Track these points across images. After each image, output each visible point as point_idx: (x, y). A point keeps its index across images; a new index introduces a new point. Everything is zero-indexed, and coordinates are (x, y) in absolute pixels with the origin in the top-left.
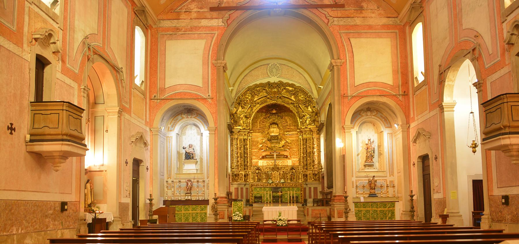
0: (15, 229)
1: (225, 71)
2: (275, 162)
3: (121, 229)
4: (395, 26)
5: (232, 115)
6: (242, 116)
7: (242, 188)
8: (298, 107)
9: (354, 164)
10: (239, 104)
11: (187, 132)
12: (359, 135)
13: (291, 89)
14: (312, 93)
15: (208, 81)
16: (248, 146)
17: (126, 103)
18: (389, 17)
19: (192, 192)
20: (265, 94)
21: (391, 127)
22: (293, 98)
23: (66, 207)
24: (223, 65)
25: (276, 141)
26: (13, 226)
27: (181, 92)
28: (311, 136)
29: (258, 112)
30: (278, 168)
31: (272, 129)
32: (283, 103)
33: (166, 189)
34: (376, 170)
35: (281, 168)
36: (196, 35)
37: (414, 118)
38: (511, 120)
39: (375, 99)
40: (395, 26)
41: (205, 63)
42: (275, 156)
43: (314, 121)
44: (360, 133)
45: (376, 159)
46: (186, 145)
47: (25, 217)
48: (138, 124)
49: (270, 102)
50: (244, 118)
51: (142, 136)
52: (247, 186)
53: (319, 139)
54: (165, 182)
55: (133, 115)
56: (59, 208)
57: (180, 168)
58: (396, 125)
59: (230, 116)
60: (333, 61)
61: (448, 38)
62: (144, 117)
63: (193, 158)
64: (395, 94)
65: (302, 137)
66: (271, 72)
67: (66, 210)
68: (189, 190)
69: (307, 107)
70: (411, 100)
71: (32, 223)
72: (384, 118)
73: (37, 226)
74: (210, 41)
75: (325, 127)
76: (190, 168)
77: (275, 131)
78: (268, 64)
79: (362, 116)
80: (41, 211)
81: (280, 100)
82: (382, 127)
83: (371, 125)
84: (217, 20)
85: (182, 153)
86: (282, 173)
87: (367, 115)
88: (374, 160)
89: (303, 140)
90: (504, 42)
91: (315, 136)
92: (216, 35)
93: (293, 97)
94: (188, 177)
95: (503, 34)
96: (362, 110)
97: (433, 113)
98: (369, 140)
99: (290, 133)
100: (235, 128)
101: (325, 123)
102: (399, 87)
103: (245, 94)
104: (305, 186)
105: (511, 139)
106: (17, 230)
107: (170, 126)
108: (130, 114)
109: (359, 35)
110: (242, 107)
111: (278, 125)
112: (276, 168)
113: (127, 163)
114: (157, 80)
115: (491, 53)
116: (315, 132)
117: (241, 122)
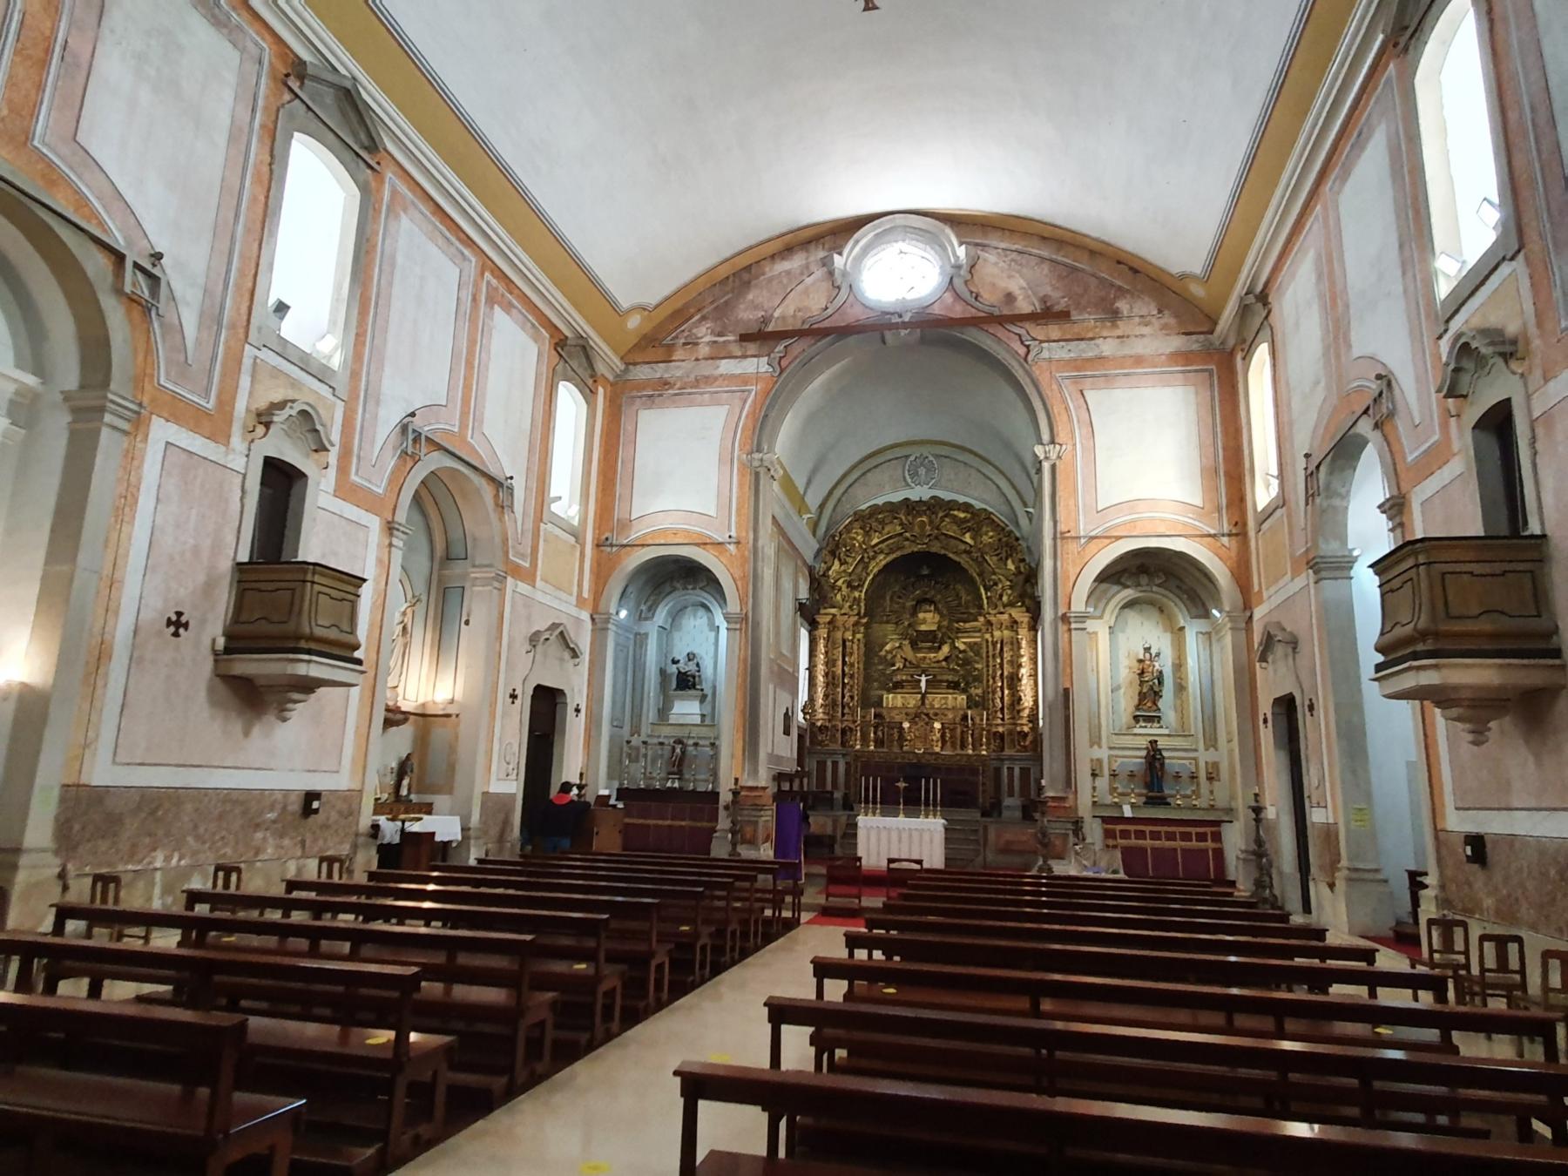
3: (292, 885)
6: (839, 583)
7: (835, 764)
8: (980, 562)
9: (1103, 711)
10: (833, 554)
11: (684, 622)
12: (1121, 637)
13: (962, 515)
17: (523, 556)
19: (685, 771)
21: (1206, 615)
22: (968, 538)
23: (315, 805)
26: (154, 850)
27: (666, 529)
31: (921, 615)
34: (1166, 732)
37: (1260, 591)
40: (1208, 353)
41: (726, 459)
42: (923, 684)
44: (1123, 631)
45: (1167, 702)
46: (681, 657)
47: (196, 827)
49: (910, 548)
55: (539, 583)
56: (295, 806)
57: (663, 712)
58: (1215, 612)
61: (1323, 384)
62: (575, 589)
66: (914, 474)
67: (316, 811)
68: (678, 764)
71: (214, 843)
72: (1185, 592)
73: (228, 851)
74: (737, 410)
76: (687, 709)
80: (244, 813)
82: (1180, 617)
83: (1156, 614)
86: (937, 725)
87: (1139, 585)
88: (1160, 704)
91: (1023, 634)
94: (678, 733)
96: (1125, 570)
97: (1300, 582)
98: (1147, 650)
103: (848, 529)
105: (1445, 672)
106: (168, 859)
107: (644, 608)
108: (532, 582)
109: (1108, 381)
113: (514, 696)
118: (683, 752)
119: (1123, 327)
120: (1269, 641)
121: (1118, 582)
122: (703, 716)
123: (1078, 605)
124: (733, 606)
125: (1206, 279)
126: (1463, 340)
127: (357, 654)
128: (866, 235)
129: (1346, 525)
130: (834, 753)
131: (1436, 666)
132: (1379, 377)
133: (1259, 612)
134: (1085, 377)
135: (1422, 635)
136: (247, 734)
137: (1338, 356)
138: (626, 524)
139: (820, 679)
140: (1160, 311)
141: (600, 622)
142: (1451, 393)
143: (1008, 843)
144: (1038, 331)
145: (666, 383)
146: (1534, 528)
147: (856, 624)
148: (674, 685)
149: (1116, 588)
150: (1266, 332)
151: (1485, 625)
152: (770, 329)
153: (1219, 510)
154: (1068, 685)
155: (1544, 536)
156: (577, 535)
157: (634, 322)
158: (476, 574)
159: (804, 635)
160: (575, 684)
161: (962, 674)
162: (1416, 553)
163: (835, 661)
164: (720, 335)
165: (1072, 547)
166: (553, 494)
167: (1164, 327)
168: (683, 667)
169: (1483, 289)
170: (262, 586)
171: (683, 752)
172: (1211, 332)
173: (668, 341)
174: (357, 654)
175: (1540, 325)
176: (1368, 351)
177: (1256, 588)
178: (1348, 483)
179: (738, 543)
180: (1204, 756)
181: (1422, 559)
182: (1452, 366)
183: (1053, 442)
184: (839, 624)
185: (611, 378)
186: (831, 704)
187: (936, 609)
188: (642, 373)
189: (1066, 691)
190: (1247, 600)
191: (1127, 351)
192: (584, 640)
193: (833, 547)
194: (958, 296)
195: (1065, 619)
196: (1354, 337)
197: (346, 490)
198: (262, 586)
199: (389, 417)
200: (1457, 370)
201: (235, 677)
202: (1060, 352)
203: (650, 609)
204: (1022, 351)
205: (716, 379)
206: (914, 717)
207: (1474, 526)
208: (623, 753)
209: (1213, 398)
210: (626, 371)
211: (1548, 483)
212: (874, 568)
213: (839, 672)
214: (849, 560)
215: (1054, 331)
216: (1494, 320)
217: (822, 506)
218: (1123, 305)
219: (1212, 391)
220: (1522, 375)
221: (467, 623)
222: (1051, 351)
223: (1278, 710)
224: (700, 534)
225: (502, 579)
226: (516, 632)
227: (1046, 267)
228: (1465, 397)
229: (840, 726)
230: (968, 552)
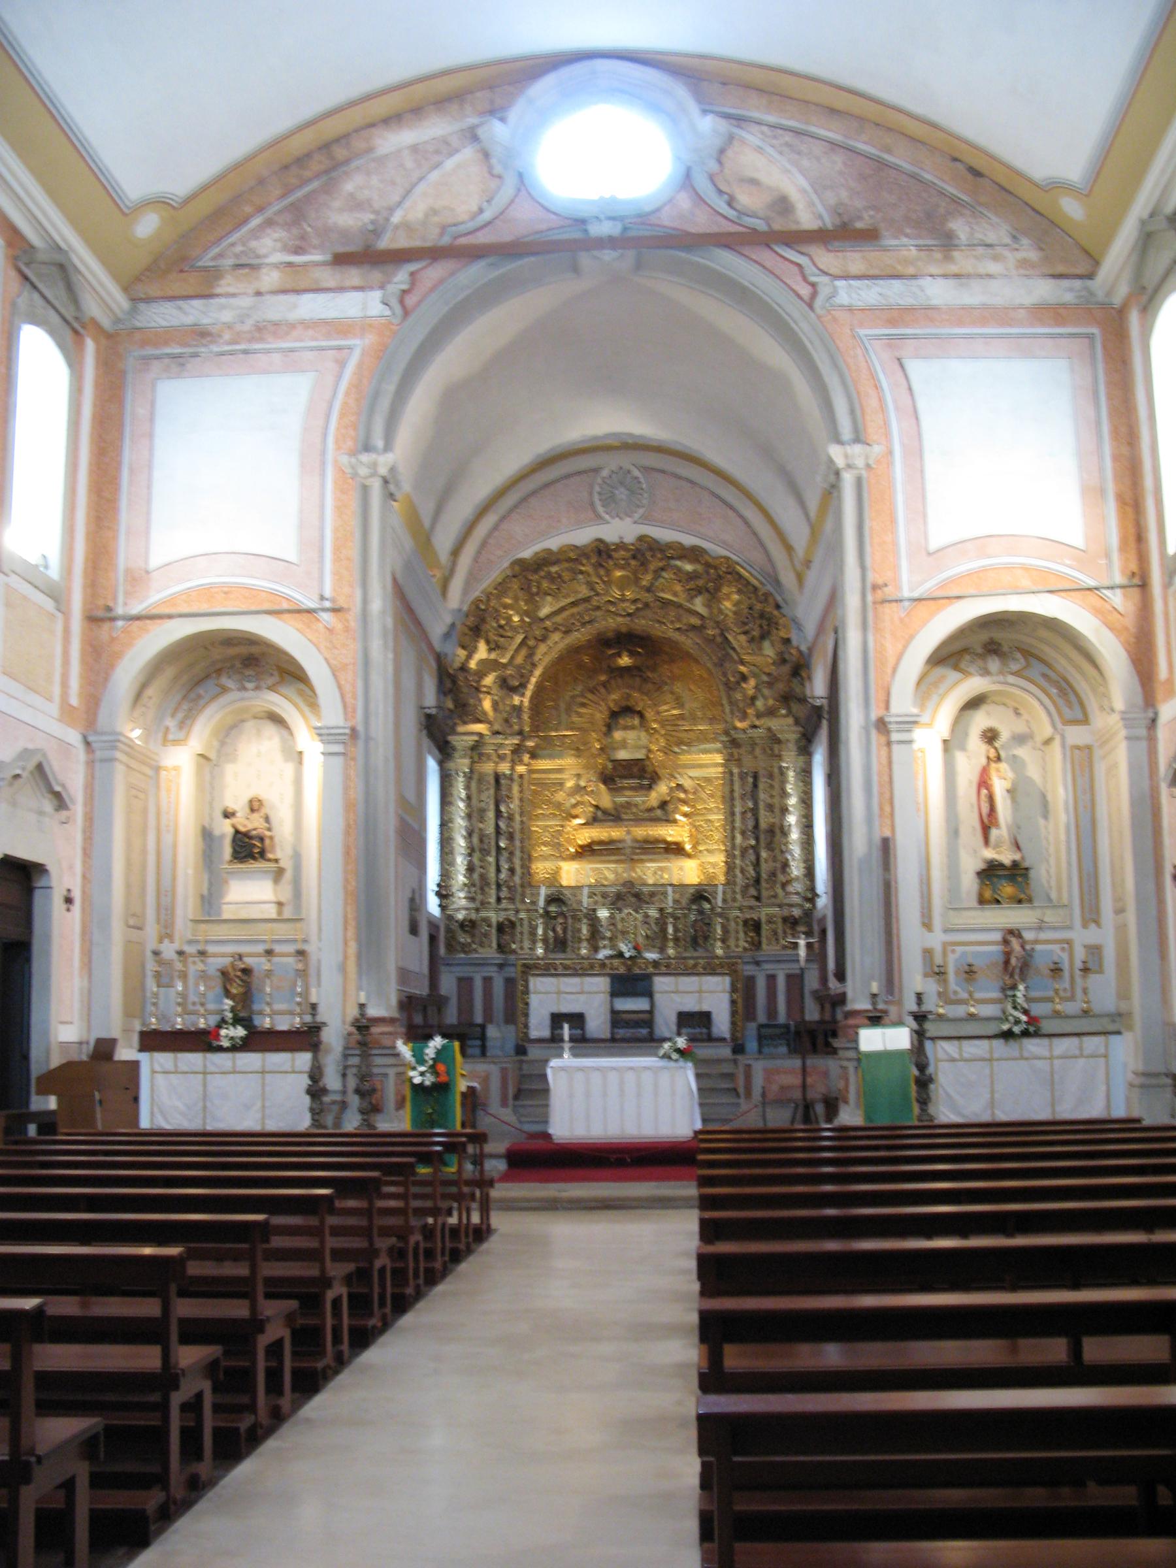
6: (489, 680)
7: (487, 981)
13: (689, 567)
14: (777, 582)
15: (322, 537)
16: (514, 805)
20: (584, 592)
22: (699, 605)
30: (637, 896)
31: (618, 735)
33: (151, 985)
35: (652, 894)
43: (787, 699)
48: (26, 715)
51: (40, 767)
52: (510, 972)
53: (806, 775)
54: (149, 954)
57: (210, 900)
59: (441, 682)
62: (57, 690)
63: (263, 854)
64: (1092, 583)
76: (250, 893)
78: (596, 470)
85: (222, 836)
86: (653, 913)
89: (743, 776)
96: (965, 650)
102: (1108, 556)
104: (749, 970)
107: (171, 723)
110: (488, 642)
112: (630, 896)
116: (792, 746)
121: (956, 667)
122: (280, 904)
123: (902, 703)
124: (332, 714)
125: (1084, 194)
128: (543, 88)
130: (483, 963)
134: (903, 337)
138: (138, 579)
139: (460, 842)
140: (1014, 238)
141: (99, 745)
143: (783, 1088)
144: (826, 258)
147: (517, 750)
148: (227, 851)
149: (954, 675)
152: (384, 243)
154: (887, 833)
156: (57, 594)
157: (147, 226)
159: (432, 765)
163: (482, 811)
164: (298, 250)
165: (890, 613)
167: (1024, 263)
172: (1090, 276)
173: (206, 261)
180: (1082, 937)
183: (858, 439)
184: (489, 750)
185: (106, 323)
186: (478, 884)
192: (72, 777)
194: (699, 199)
195: (882, 725)
202: (869, 294)
204: (805, 291)
205: (292, 326)
210: (134, 311)
212: (546, 654)
213: (490, 830)
215: (855, 259)
217: (456, 552)
218: (960, 227)
222: (852, 290)
224: (272, 594)
227: (839, 159)
229: (494, 917)
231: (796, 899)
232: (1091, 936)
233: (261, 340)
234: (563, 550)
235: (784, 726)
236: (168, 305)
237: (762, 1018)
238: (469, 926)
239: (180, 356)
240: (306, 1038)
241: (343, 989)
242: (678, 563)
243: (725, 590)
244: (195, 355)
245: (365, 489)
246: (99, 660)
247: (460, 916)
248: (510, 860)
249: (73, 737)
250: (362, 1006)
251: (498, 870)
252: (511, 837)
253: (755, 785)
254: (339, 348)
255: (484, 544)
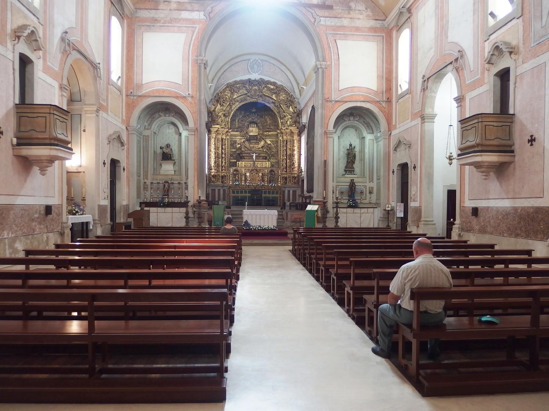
0: (5, 233)
1: (205, 68)
2: (254, 164)
4: (381, 29)
5: (210, 113)
6: (220, 114)
7: (219, 190)
8: (279, 107)
10: (218, 101)
12: (341, 140)
13: (272, 87)
17: (104, 100)
18: (377, 20)
20: (245, 92)
22: (274, 97)
24: (204, 62)
25: (254, 141)
26: (4, 230)
28: (291, 138)
29: (237, 110)
31: (251, 129)
32: (263, 102)
36: (176, 28)
37: (395, 125)
38: (484, 138)
39: (359, 104)
40: (381, 29)
42: (254, 157)
43: (295, 122)
47: (15, 221)
48: (115, 122)
49: (249, 100)
50: (222, 116)
51: (119, 136)
53: (300, 141)
55: (110, 113)
56: (43, 212)
59: (208, 114)
60: (318, 63)
61: (433, 50)
65: (283, 138)
69: (288, 107)
70: (394, 106)
71: (21, 227)
72: (366, 124)
73: (25, 230)
75: (306, 130)
76: (168, 168)
77: (253, 131)
78: (249, 60)
79: (345, 121)
80: (28, 215)
81: (260, 98)
84: (198, 13)
86: (260, 174)
87: (350, 120)
89: (283, 141)
90: (485, 61)
91: (296, 137)
92: (197, 28)
93: (274, 96)
94: (166, 178)
95: (484, 53)
96: (345, 115)
99: (270, 133)
100: (213, 126)
101: (307, 125)
102: (383, 93)
103: (224, 91)
105: (483, 157)
106: (8, 234)
110: (220, 104)
111: (257, 124)
113: (104, 164)
114: (133, 75)
115: (472, 69)
117: (220, 120)
118: (169, 187)
119: (353, 14)
120: (399, 143)
126: (496, 45)
127: (69, 146)
129: (434, 103)
131: (481, 155)
132: (459, 51)
133: (394, 133)
135: (478, 145)
136: (25, 181)
137: (442, 40)
140: (366, 9)
142: (489, 63)
143: (295, 218)
145: (156, 20)
146: (511, 111)
147: (227, 132)
150: (408, 24)
151: (495, 142)
153: (383, 93)
155: (514, 115)
158: (86, 108)
160: (121, 156)
161: (268, 154)
162: (478, 118)
166: (112, 70)
168: (165, 150)
169: (505, 27)
170: (28, 115)
171: (169, 187)
174: (69, 146)
175: (524, 44)
176: (455, 40)
177: (394, 124)
178: (437, 88)
179: (192, 97)
181: (480, 120)
182: (491, 53)
186: (217, 165)
187: (257, 126)
188: (144, 14)
189: (325, 161)
190: (390, 127)
191: (353, 25)
192: (124, 138)
193: (218, 99)
195: (326, 133)
196: (450, 34)
197: (47, 70)
198: (28, 115)
199: (58, 33)
200: (492, 55)
201: (20, 156)
202: (330, 22)
203: (149, 125)
204: (313, 20)
205: (180, 20)
206: (251, 171)
207: (489, 109)
208: (141, 187)
209: (383, 48)
211: (518, 97)
214: (225, 105)
215: (326, 13)
216: (508, 39)
218: (352, 5)
219: (383, 45)
220: (515, 60)
221: (84, 131)
223: (399, 168)
224: (175, 92)
225: (98, 111)
226: (104, 136)
228: (492, 64)
230: (274, 103)
231: (296, 172)
232: (371, 185)
233: (171, 23)
234: (241, 81)
235: (294, 129)
236: (146, 11)
237: (291, 201)
238: (214, 176)
239: (149, 26)
240: (184, 204)
241: (194, 193)
242: (269, 86)
243: (281, 93)
244: (154, 26)
245: (200, 66)
246: (130, 107)
247: (213, 174)
248: (225, 160)
249: (124, 128)
250: (200, 197)
251: (222, 163)
252: (225, 154)
253: (287, 144)
254: (193, 27)
255: (220, 78)
